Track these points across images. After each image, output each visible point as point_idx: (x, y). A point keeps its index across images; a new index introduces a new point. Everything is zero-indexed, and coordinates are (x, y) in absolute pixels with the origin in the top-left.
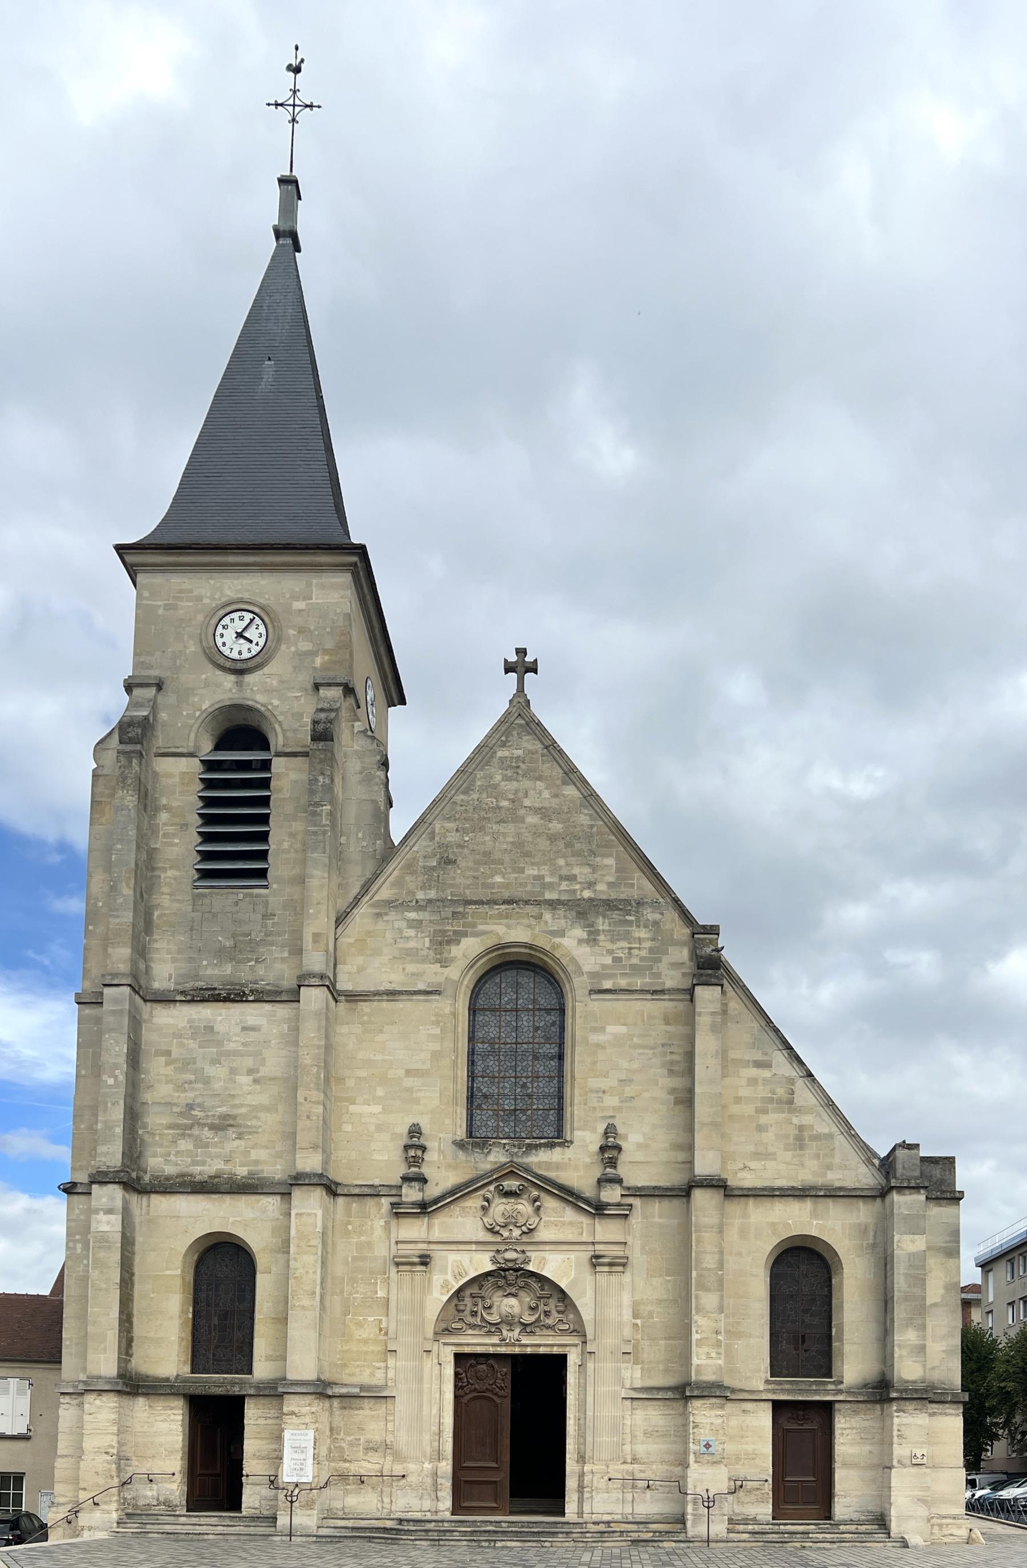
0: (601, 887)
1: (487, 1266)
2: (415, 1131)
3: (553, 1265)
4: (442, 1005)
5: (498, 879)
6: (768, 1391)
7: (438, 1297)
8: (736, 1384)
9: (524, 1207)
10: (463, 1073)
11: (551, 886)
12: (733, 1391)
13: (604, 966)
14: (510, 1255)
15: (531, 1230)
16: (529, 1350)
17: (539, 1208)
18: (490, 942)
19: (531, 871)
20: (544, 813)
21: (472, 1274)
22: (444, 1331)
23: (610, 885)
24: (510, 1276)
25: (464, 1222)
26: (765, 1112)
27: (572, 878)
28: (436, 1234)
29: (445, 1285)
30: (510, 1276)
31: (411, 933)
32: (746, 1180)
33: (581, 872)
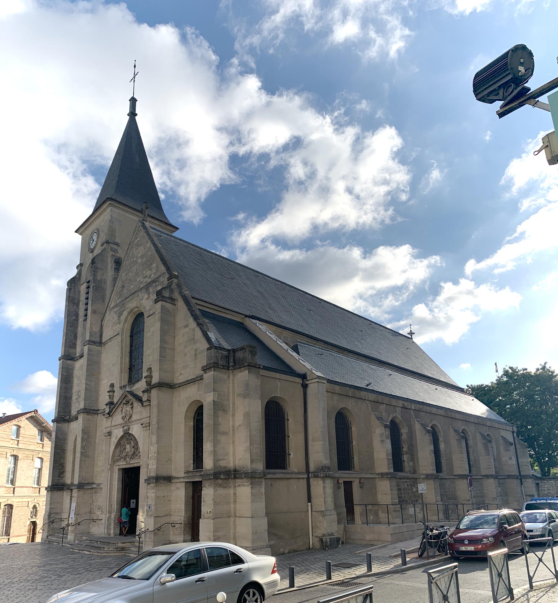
0: (152, 276)
1: (122, 434)
2: (112, 385)
3: (136, 430)
4: (119, 338)
5: (132, 287)
6: (188, 477)
7: (113, 447)
8: (177, 475)
9: (128, 408)
10: (128, 359)
11: (142, 282)
12: (175, 478)
13: (151, 306)
14: (125, 428)
15: (130, 417)
16: (132, 466)
17: (132, 408)
18: (128, 310)
19: (138, 280)
20: (142, 257)
21: (119, 437)
22: (114, 461)
23: (155, 273)
24: (127, 436)
25: (118, 418)
26: (186, 347)
27: (145, 277)
28: (113, 424)
29: (114, 443)
30: (127, 436)
31: (115, 316)
32: (180, 379)
33: (148, 273)
